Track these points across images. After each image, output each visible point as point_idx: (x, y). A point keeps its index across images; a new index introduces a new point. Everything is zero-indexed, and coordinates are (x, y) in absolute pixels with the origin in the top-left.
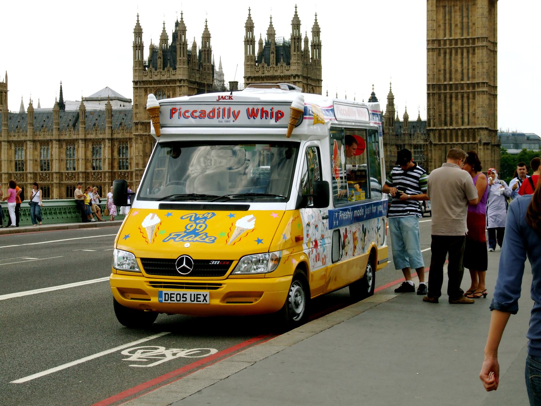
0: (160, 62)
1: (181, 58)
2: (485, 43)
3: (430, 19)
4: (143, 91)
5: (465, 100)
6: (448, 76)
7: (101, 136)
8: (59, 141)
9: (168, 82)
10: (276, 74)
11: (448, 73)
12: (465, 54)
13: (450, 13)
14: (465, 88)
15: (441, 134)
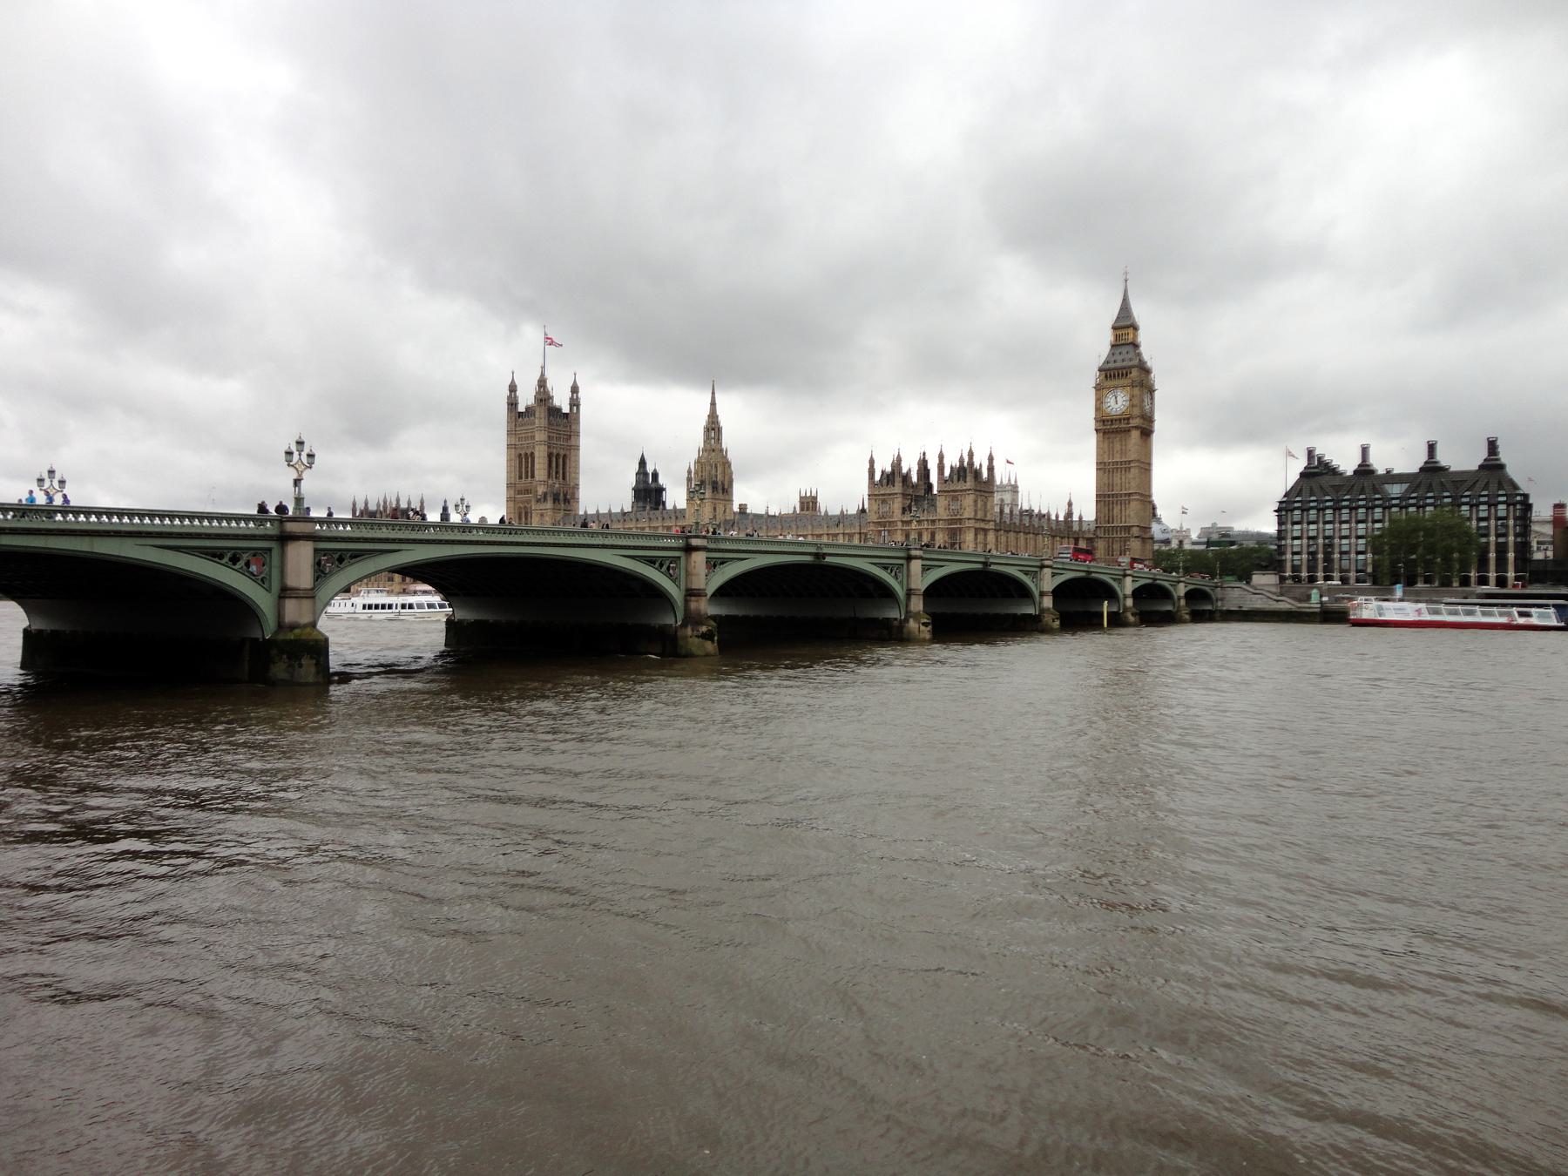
0: (885, 481)
1: (898, 480)
2: (1136, 464)
3: (1098, 447)
4: (874, 501)
5: (1123, 506)
6: (1111, 488)
7: (853, 531)
8: (828, 534)
9: (890, 495)
10: (957, 488)
11: (1111, 486)
12: (1123, 472)
13: (1113, 442)
14: (1124, 498)
15: (1106, 530)
